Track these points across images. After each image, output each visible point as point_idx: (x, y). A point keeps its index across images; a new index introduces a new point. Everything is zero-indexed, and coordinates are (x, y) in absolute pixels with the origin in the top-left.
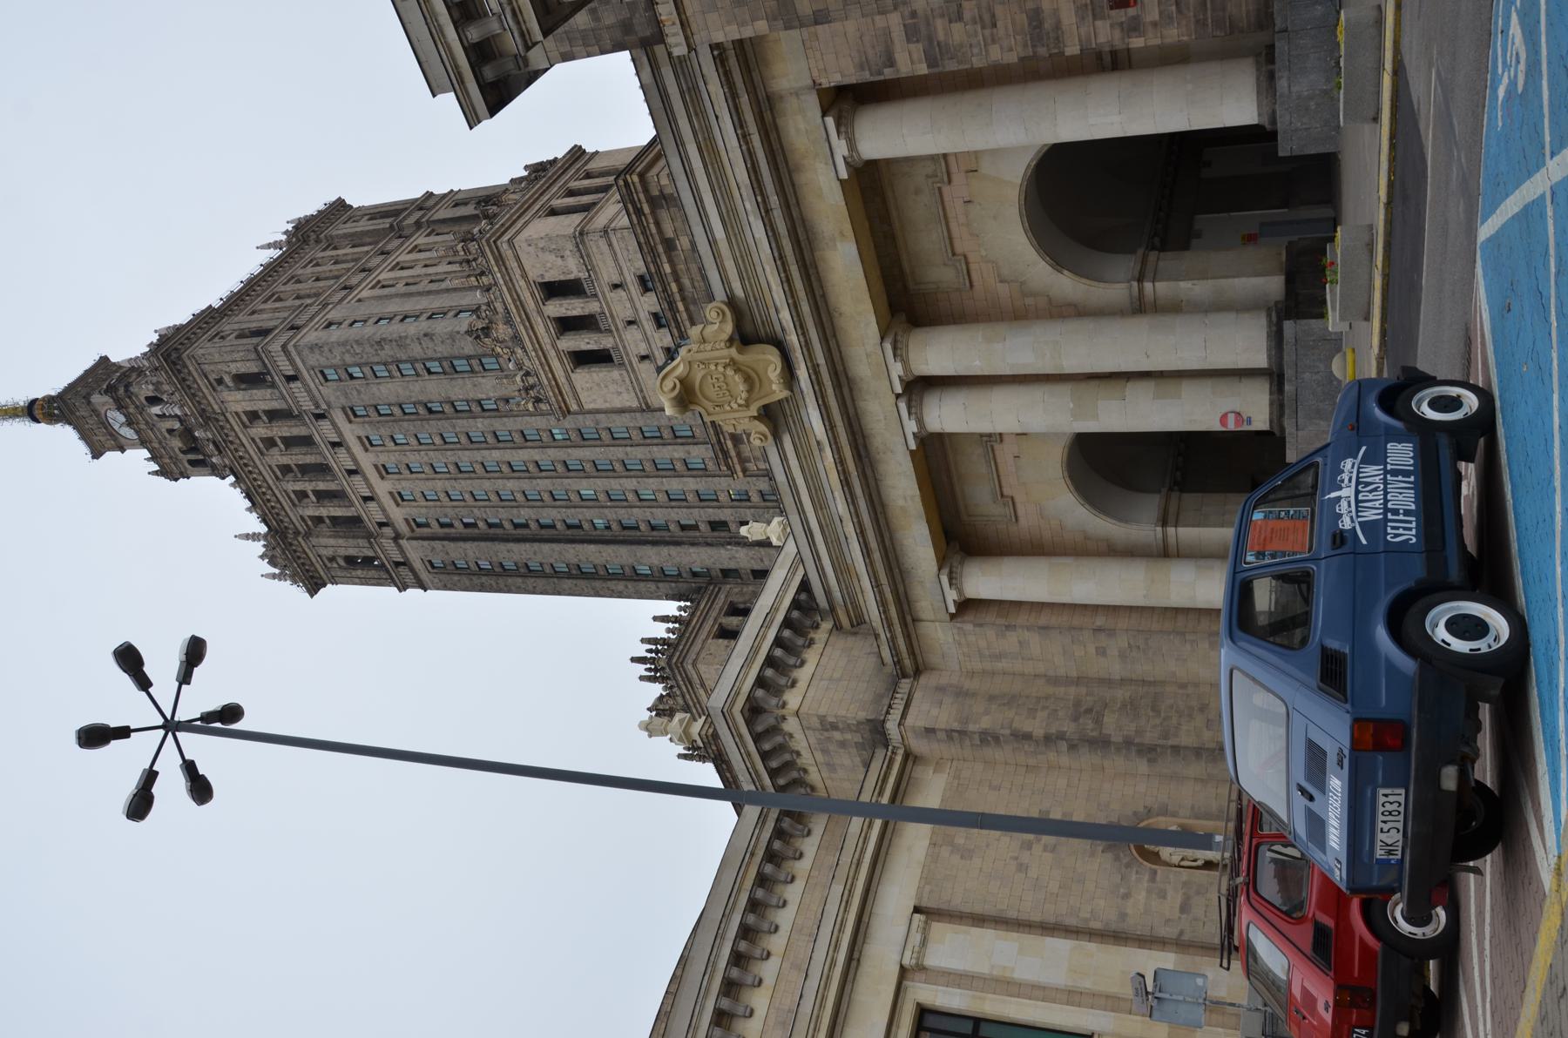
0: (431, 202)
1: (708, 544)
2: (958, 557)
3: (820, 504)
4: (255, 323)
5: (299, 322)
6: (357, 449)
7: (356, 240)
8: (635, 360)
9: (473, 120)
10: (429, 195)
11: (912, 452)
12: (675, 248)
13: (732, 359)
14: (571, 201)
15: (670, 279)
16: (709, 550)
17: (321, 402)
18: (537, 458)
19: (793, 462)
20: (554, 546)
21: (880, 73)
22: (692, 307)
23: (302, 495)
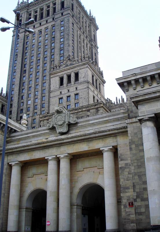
0: (96, 48)
1: (18, 101)
2: (21, 165)
3: (34, 137)
4: (75, 8)
5: (74, 17)
6: (46, 26)
7: (90, 31)
8: (60, 91)
9: (117, 79)
10: (98, 48)
11: (45, 157)
12: (88, 112)
13: (65, 122)
14: (95, 80)
15: (82, 110)
16: (17, 102)
17: (57, 20)
18: (40, 66)
19: (43, 132)
20: (20, 67)
21: (120, 158)
22: (76, 114)
23: (36, 12)
